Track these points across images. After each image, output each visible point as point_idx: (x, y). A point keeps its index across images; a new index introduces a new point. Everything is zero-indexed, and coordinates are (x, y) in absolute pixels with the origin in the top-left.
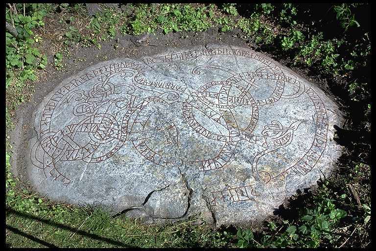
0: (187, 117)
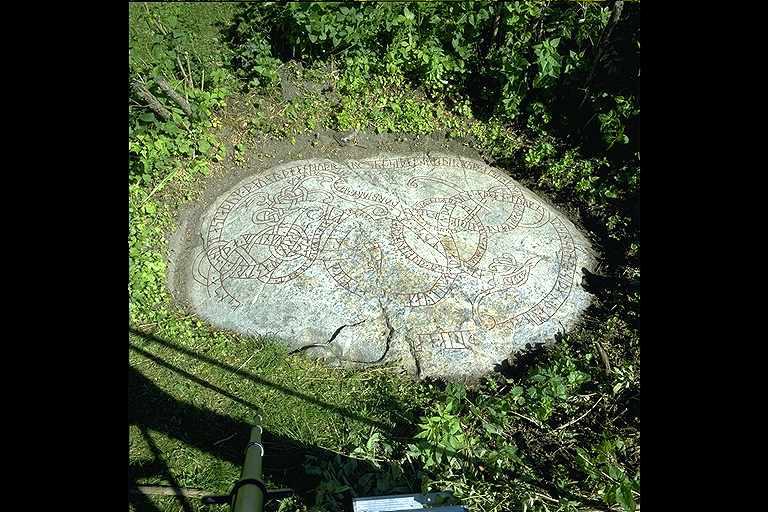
0: (396, 238)
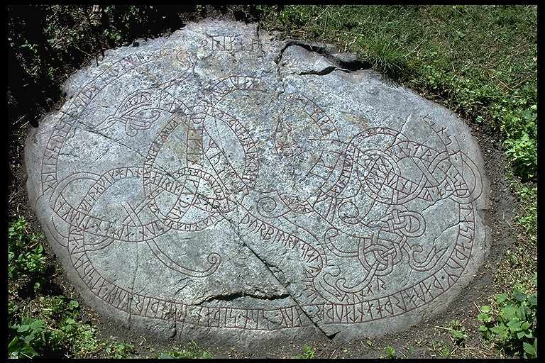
0: (255, 160)
